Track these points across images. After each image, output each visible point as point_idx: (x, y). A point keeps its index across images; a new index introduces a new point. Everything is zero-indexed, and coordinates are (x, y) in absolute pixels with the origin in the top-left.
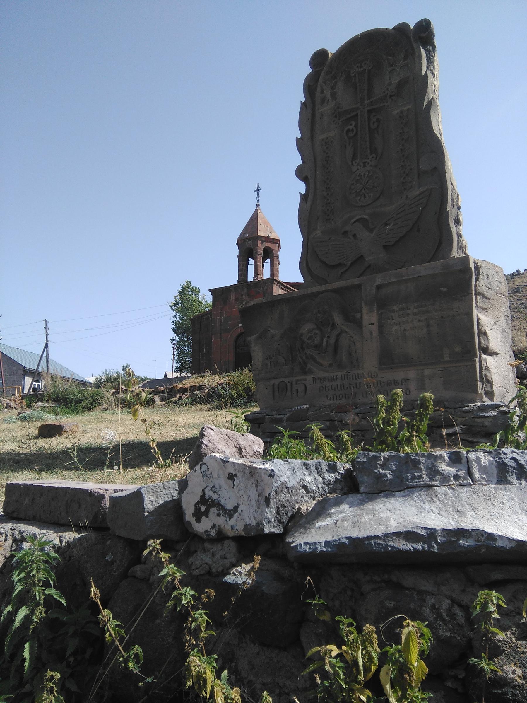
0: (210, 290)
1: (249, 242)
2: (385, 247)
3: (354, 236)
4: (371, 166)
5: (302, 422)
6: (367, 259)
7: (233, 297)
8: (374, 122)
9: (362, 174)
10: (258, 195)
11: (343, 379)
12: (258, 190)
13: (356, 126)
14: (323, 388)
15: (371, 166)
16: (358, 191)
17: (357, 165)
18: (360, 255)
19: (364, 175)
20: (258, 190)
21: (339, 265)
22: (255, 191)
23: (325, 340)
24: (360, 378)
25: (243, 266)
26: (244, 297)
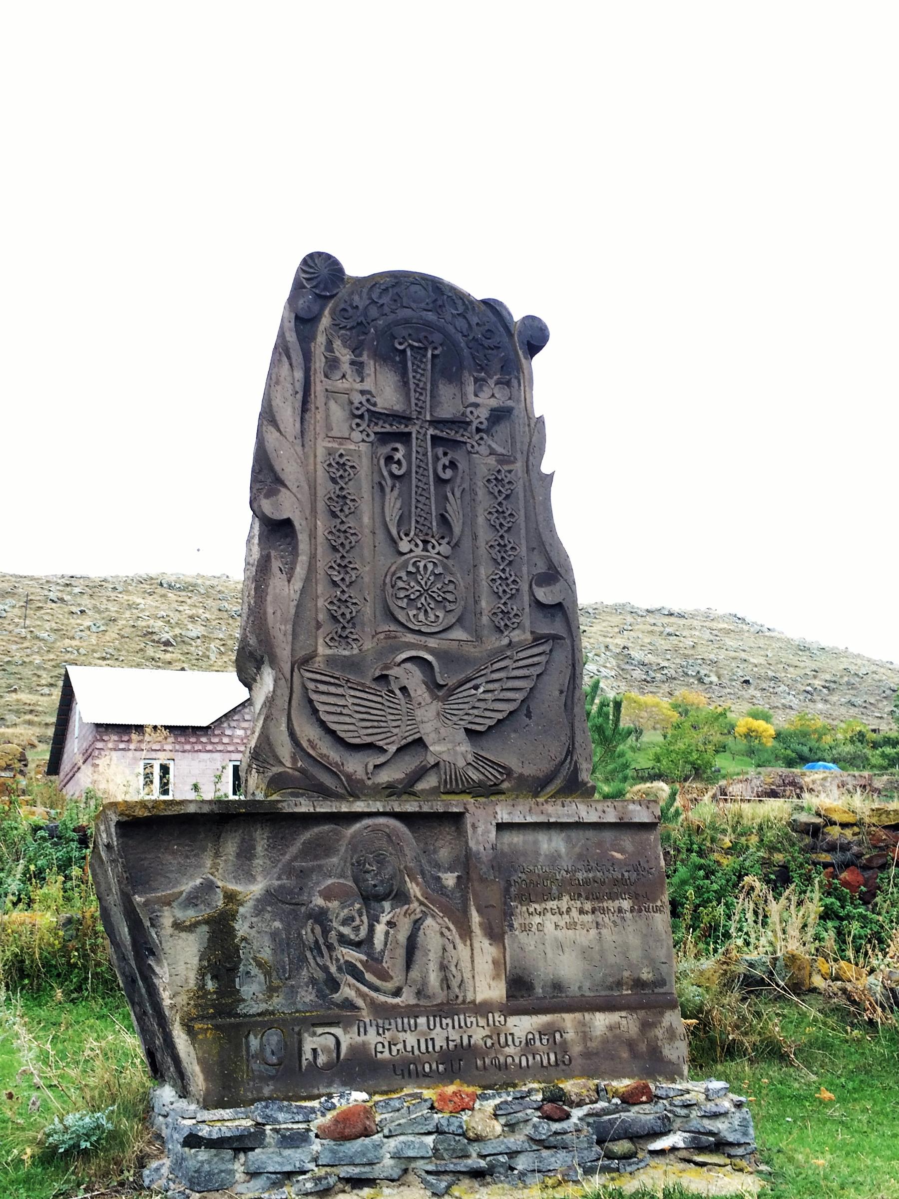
2: (466, 729)
3: (404, 689)
4: (438, 553)
5: (367, 1139)
6: (431, 748)
8: (445, 467)
9: (421, 565)
11: (432, 1027)
13: (408, 456)
14: (384, 1047)
15: (438, 553)
16: (412, 597)
17: (410, 542)
18: (417, 736)
19: (425, 567)
21: (370, 746)
23: (380, 929)
24: (469, 1025)
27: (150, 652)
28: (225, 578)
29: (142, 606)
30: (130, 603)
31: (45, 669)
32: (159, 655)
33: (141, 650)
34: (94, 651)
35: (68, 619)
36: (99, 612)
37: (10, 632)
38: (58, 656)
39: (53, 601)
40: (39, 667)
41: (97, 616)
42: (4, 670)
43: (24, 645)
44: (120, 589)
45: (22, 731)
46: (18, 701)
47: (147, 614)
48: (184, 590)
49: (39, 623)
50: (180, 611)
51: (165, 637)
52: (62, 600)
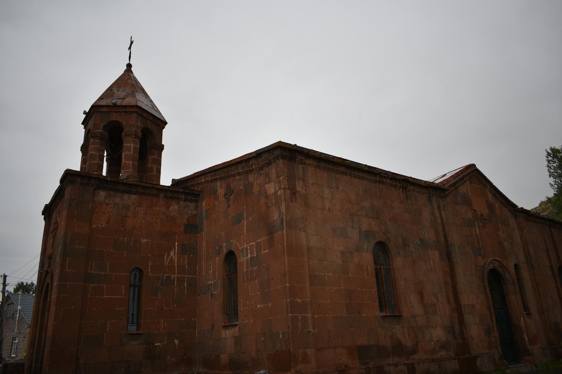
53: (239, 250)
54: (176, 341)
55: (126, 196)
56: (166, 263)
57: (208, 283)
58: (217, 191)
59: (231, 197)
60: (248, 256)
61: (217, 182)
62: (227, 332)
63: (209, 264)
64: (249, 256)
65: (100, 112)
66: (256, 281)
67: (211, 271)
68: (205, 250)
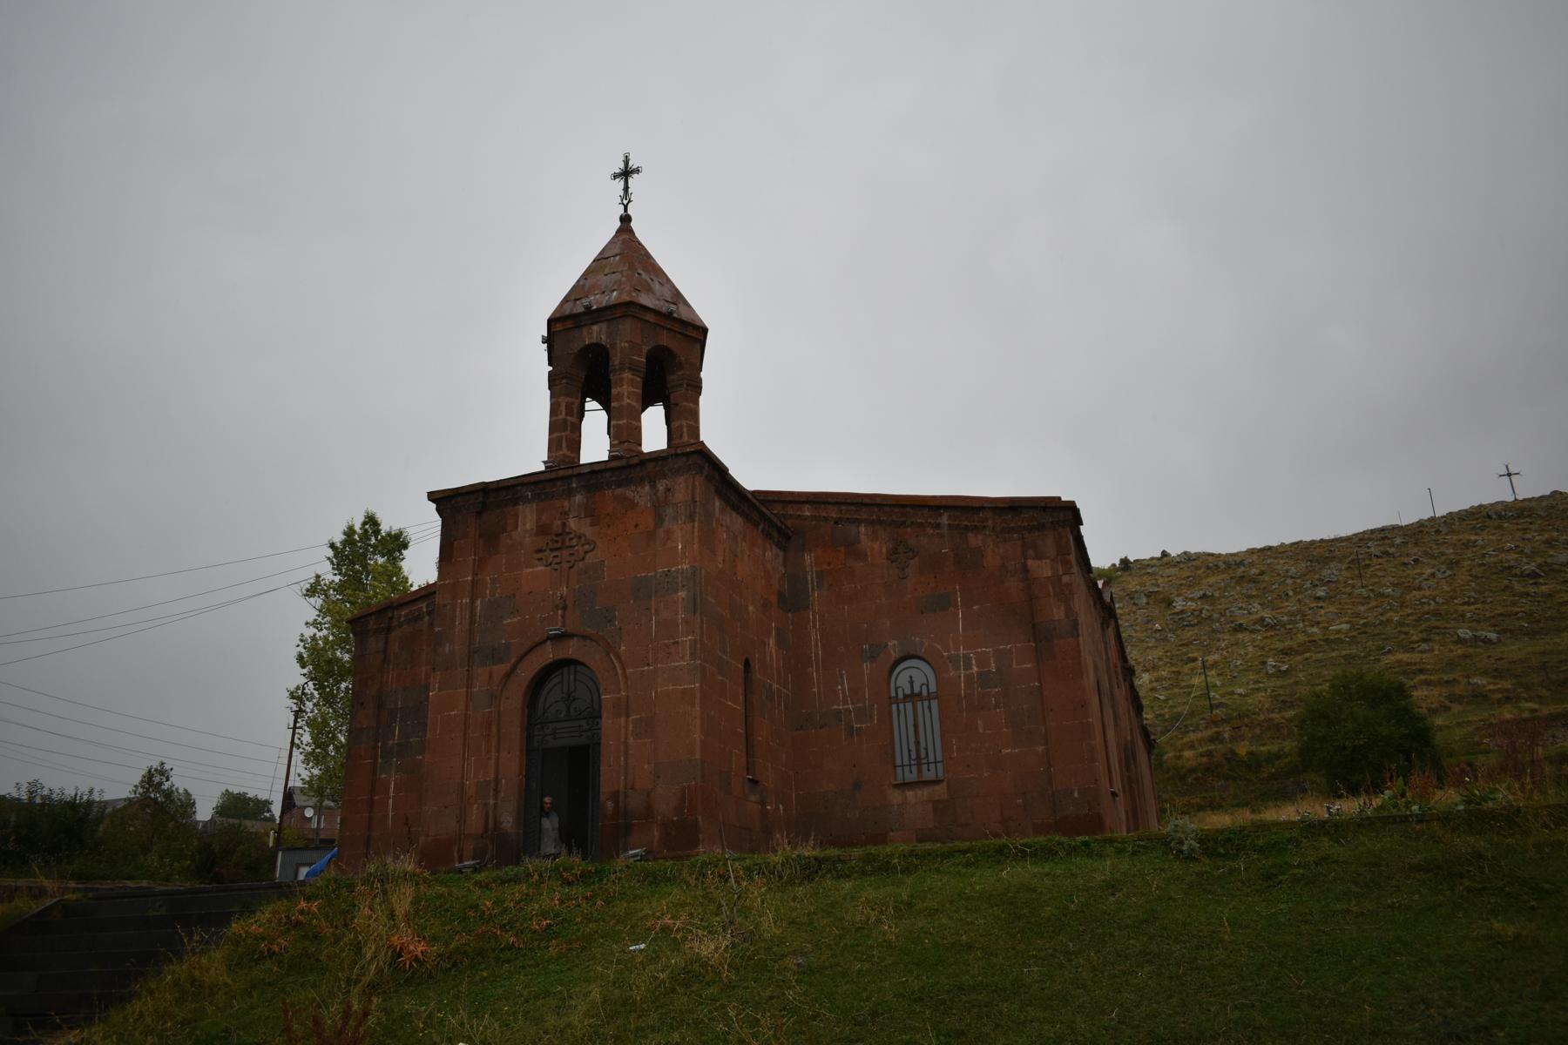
0: (433, 497)
1: (595, 328)
7: (527, 518)
10: (626, 189)
12: (626, 173)
20: (626, 173)
22: (615, 176)
25: (569, 412)
26: (573, 524)
27: (1518, 587)
28: (1558, 496)
29: (1480, 542)
30: (1465, 541)
31: (1408, 625)
32: (1532, 590)
33: (1507, 587)
34: (1453, 598)
35: (1404, 571)
36: (1433, 557)
37: (1350, 594)
38: (1415, 609)
39: (1377, 556)
40: (1401, 624)
41: (1433, 562)
42: (1365, 633)
43: (1370, 606)
44: (1444, 530)
45: (1426, 693)
46: (1399, 661)
47: (1492, 549)
48: (1519, 517)
49: (1377, 580)
50: (1528, 540)
51: (1532, 567)
52: (1387, 553)
53: (942, 656)
54: (781, 806)
55: (734, 514)
56: (768, 658)
57: (835, 707)
58: (859, 542)
59: (912, 562)
60: (972, 669)
61: (858, 526)
62: (910, 794)
63: (838, 673)
64: (975, 669)
65: (641, 319)
66: (998, 710)
67: (842, 684)
68: (817, 645)
